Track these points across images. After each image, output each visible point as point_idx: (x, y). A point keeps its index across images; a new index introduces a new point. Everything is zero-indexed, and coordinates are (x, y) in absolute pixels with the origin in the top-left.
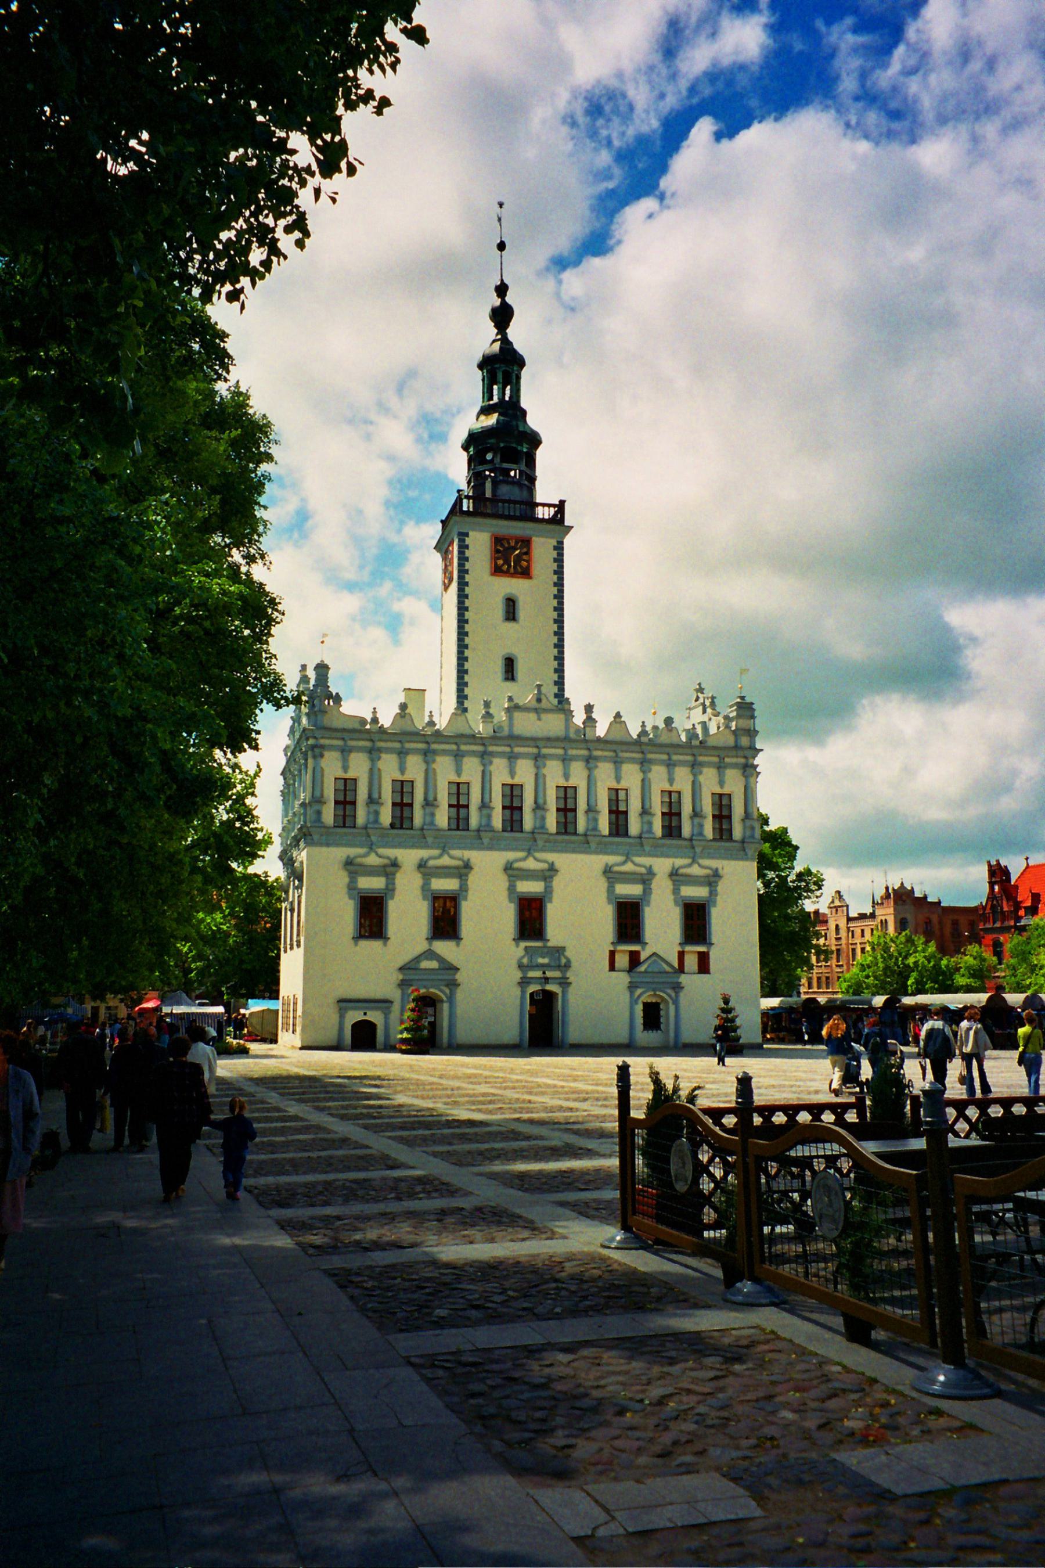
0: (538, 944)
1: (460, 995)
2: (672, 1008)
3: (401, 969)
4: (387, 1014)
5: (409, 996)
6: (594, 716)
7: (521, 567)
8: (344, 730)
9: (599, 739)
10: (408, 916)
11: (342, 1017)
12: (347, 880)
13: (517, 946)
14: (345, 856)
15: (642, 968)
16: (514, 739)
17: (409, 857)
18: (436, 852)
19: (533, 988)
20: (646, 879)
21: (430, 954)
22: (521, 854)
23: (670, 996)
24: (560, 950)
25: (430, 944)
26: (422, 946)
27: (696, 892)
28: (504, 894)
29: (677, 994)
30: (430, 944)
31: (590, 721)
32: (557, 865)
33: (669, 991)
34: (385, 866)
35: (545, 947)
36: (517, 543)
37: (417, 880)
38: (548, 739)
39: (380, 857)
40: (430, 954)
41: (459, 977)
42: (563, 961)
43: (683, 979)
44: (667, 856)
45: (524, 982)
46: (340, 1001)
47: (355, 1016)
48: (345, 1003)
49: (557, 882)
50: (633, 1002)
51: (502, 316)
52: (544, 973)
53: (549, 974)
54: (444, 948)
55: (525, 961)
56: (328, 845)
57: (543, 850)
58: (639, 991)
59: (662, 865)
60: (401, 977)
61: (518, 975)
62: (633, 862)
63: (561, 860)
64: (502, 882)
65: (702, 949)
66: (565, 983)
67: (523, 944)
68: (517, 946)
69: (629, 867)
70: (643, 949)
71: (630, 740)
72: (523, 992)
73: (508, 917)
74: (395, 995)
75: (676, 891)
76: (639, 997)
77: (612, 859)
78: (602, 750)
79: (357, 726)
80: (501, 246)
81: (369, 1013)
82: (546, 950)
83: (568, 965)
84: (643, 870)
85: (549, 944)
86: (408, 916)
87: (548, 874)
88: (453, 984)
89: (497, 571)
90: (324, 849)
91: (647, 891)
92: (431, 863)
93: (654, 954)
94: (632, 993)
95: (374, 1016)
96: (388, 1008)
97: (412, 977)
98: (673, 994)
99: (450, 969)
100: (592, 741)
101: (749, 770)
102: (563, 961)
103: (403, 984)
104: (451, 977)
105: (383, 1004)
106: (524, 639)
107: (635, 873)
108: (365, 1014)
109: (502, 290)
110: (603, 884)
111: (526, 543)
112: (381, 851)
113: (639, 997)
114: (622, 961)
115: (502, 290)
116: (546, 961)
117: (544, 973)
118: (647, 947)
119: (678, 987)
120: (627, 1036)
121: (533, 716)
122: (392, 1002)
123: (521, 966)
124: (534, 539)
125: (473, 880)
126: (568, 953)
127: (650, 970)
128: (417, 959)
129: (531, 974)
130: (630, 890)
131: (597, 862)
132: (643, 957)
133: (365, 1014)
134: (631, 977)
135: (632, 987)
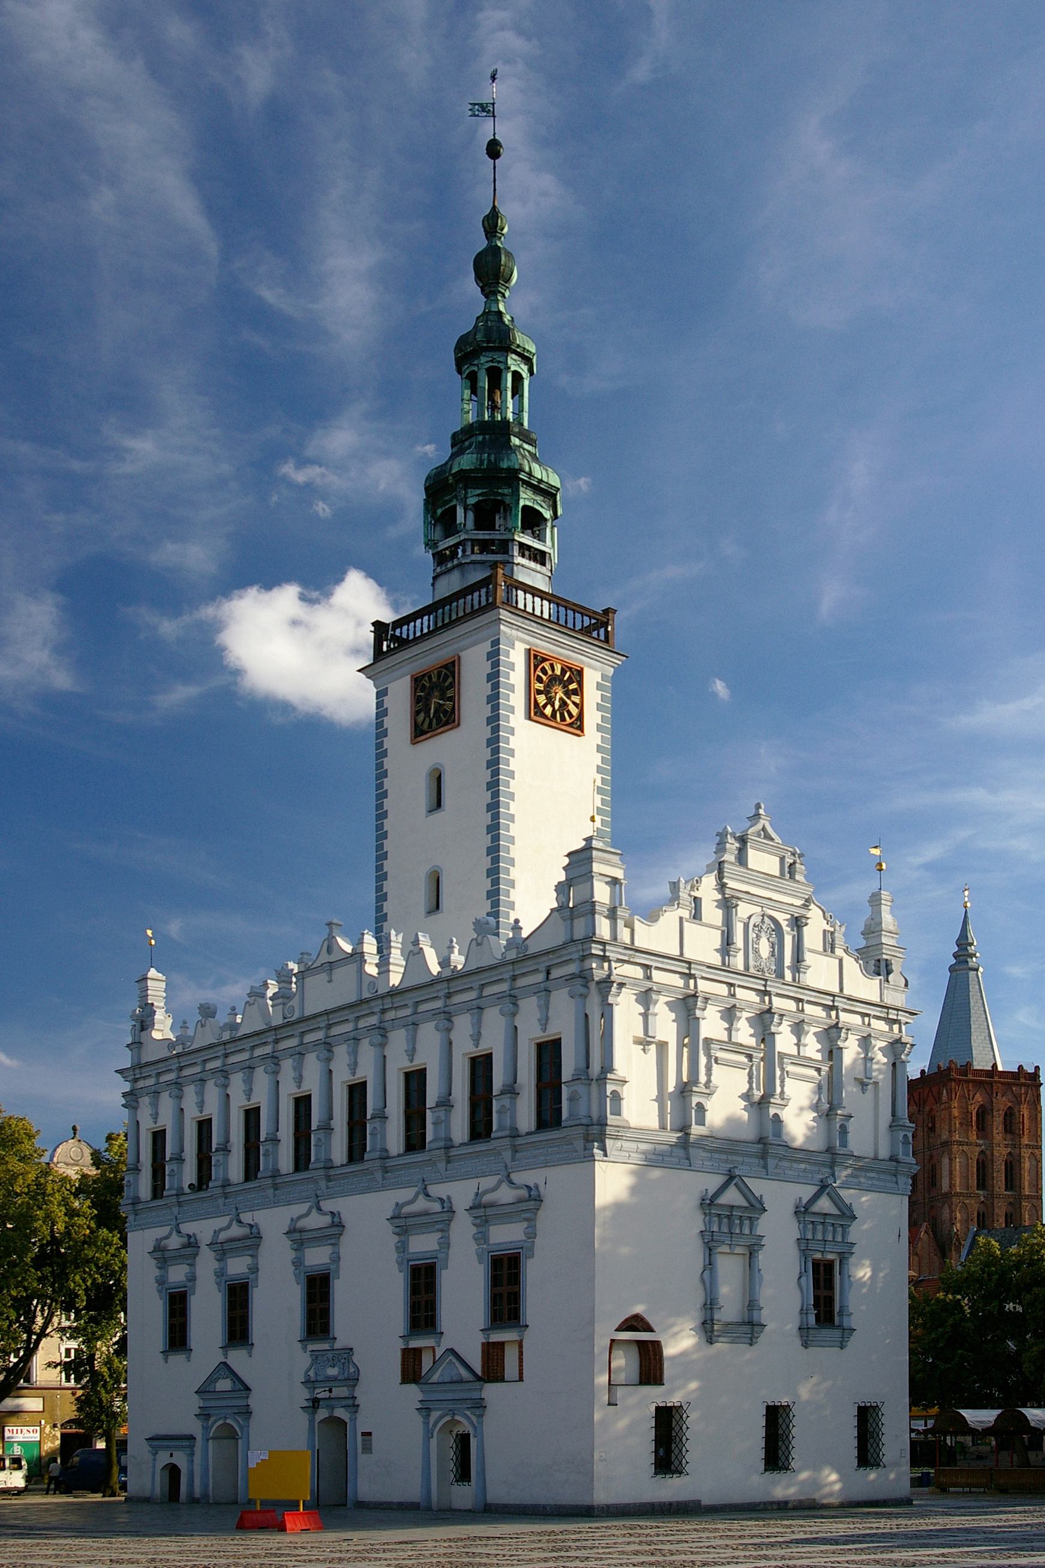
0: (326, 1346)
15: (435, 1378)
19: (322, 1414)
21: (225, 1368)
22: (303, 1208)
32: (346, 1218)
34: (184, 1247)
36: (440, 673)
42: (352, 1370)
43: (491, 1392)
47: (164, 1458)
48: (158, 1441)
50: (428, 1434)
54: (237, 1358)
57: (330, 1197)
58: (435, 1415)
59: (461, 1193)
61: (303, 1395)
66: (354, 1407)
68: (305, 1349)
69: (421, 1204)
72: (312, 1421)
74: (194, 1427)
75: (481, 1237)
77: (404, 1194)
81: (174, 1453)
82: (330, 1355)
84: (437, 1207)
85: (338, 1345)
89: (420, 732)
92: (223, 1236)
93: (452, 1351)
95: (180, 1459)
96: (192, 1447)
97: (213, 1403)
98: (474, 1419)
102: (352, 1370)
103: (204, 1415)
104: (243, 1403)
107: (426, 1213)
108: (171, 1455)
117: (330, 1391)
119: (479, 1406)
122: (192, 1438)
123: (308, 1382)
128: (212, 1379)
130: (423, 1244)
133: (171, 1455)
135: (425, 1410)
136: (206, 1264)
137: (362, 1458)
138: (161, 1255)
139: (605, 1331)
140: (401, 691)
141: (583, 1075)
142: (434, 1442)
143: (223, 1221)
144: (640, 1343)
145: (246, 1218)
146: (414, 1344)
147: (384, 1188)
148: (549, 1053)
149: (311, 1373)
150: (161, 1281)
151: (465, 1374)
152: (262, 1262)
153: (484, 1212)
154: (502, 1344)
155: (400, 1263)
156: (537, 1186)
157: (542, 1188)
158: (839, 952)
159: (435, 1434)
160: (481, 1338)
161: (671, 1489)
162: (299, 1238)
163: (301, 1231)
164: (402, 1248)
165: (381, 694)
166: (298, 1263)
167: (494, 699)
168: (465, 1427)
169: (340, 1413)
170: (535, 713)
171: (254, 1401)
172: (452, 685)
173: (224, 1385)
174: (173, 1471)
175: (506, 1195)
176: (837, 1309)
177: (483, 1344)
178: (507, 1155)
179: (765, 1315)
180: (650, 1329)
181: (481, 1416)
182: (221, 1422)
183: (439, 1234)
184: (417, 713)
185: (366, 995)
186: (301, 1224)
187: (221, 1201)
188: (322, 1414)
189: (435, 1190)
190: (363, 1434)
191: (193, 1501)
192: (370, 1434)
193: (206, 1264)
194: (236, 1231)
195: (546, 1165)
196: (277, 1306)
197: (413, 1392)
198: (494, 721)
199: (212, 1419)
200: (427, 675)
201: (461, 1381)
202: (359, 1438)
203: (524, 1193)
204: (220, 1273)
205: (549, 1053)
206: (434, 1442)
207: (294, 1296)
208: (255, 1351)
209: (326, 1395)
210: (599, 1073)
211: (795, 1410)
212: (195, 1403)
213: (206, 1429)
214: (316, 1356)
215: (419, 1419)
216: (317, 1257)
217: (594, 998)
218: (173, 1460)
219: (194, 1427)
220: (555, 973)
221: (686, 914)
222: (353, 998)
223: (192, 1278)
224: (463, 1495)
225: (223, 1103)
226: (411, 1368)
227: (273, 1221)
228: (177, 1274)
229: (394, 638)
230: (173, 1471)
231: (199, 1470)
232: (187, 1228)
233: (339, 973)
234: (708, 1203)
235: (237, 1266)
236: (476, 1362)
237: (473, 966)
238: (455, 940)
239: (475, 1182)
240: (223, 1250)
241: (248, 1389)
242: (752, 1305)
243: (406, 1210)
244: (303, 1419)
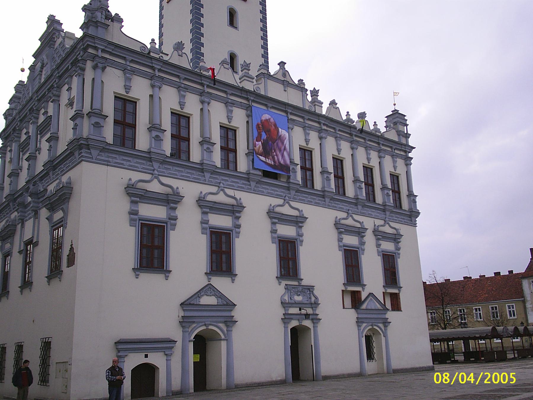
1: (237, 333)
2: (383, 339)
3: (182, 304)
5: (190, 333)
6: (319, 98)
13: (280, 283)
14: (126, 182)
15: (364, 306)
17: (190, 190)
18: (214, 189)
19: (294, 323)
20: (360, 232)
21: (209, 289)
22: (281, 202)
23: (381, 329)
24: (310, 289)
25: (209, 280)
26: (203, 281)
29: (386, 326)
30: (209, 280)
31: (316, 102)
33: (381, 325)
35: (300, 285)
37: (196, 215)
39: (162, 184)
40: (209, 289)
41: (236, 314)
46: (115, 343)
48: (124, 346)
49: (306, 230)
52: (300, 310)
54: (221, 283)
55: (286, 298)
56: (107, 164)
57: (294, 200)
58: (364, 325)
60: (182, 314)
61: (280, 312)
64: (266, 224)
65: (395, 291)
66: (315, 320)
67: (284, 283)
68: (280, 283)
70: (363, 289)
72: (286, 328)
73: (270, 254)
76: (364, 330)
78: (327, 126)
81: (149, 355)
83: (315, 305)
84: (358, 225)
85: (304, 283)
87: (299, 219)
88: (230, 322)
90: (103, 168)
91: (363, 243)
92: (210, 198)
93: (371, 294)
94: (359, 326)
95: (156, 359)
99: (227, 305)
101: (408, 161)
102: (313, 299)
105: (165, 345)
108: (146, 356)
110: (333, 234)
112: (164, 180)
113: (364, 330)
114: (348, 301)
119: (386, 323)
120: (359, 367)
121: (281, 87)
123: (284, 304)
125: (245, 220)
127: (370, 308)
128: (198, 294)
132: (364, 296)
133: (146, 356)
134: (358, 313)
135: (359, 322)
147: (329, 207)
149: (286, 298)
164: (340, 240)
169: (307, 323)
173: (208, 300)
186: (278, 209)
208: (237, 279)
212: (177, 313)
214: (287, 287)
215: (356, 328)
219: (175, 332)
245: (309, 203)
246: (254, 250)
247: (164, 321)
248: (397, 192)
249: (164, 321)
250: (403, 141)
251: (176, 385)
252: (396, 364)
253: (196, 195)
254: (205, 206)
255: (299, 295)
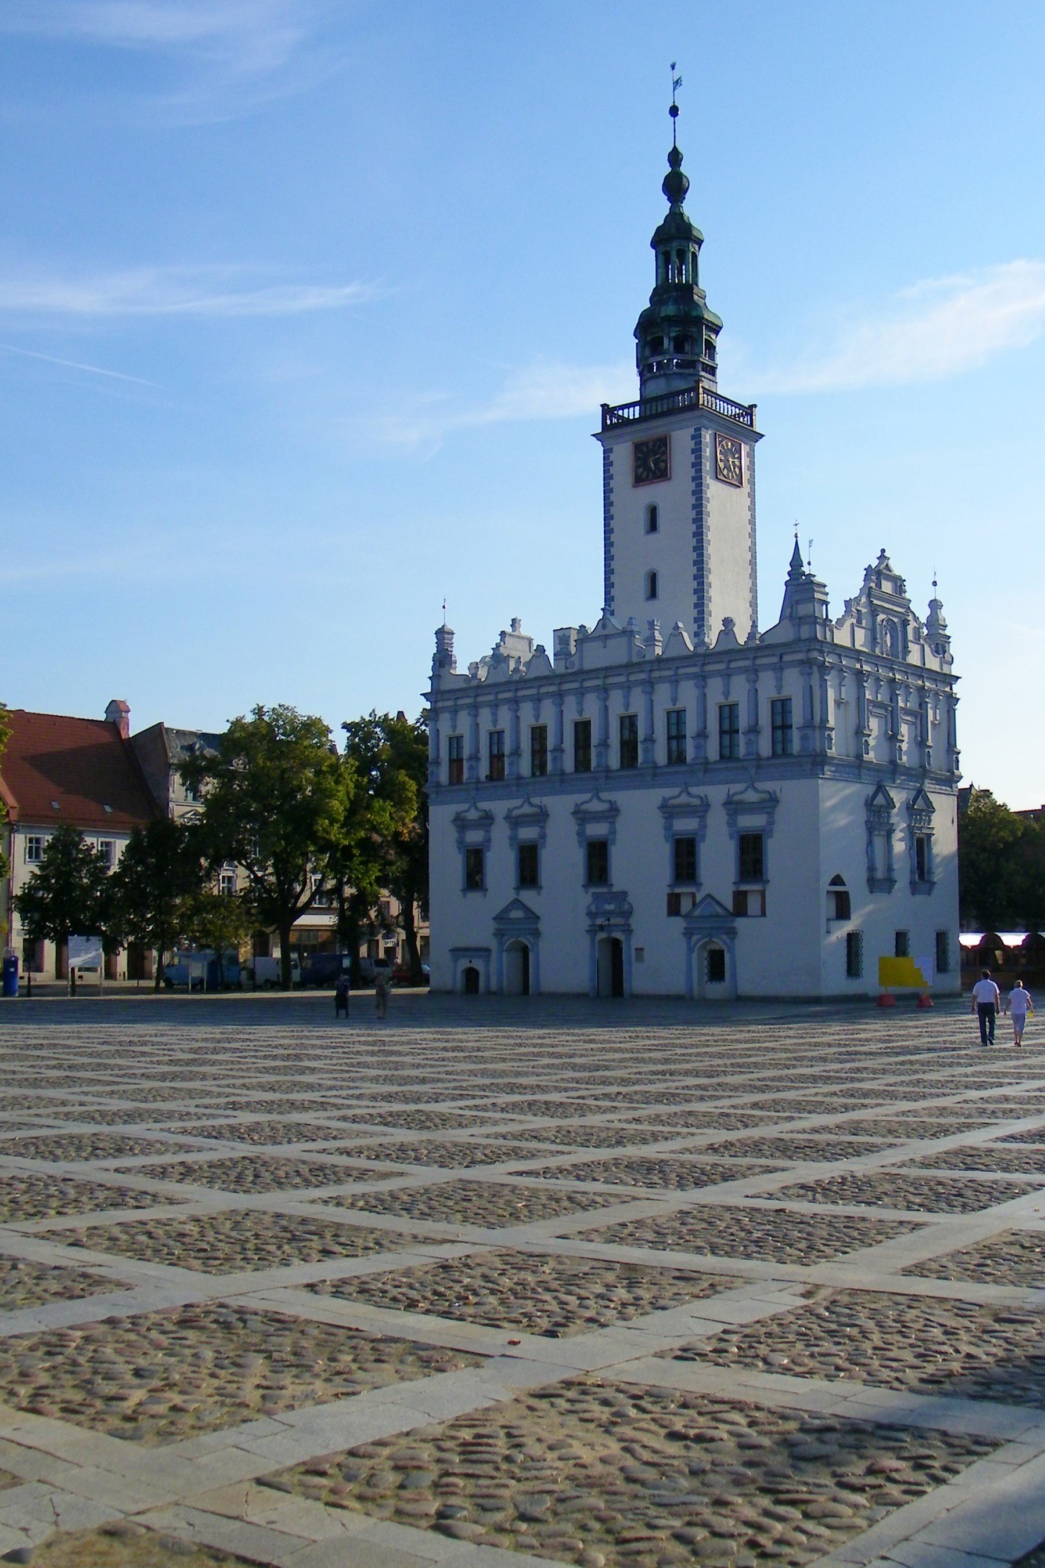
0: (605, 890)
4: (488, 962)
7: (660, 470)
8: (449, 691)
9: (659, 660)
10: (501, 865)
11: (455, 965)
12: (508, 832)
15: (697, 913)
16: (583, 674)
17: (499, 807)
19: (602, 935)
21: (517, 904)
22: (587, 796)
24: (625, 894)
25: (518, 894)
26: (512, 895)
27: (751, 822)
28: (574, 840)
29: (733, 939)
30: (518, 894)
33: (724, 937)
34: (481, 818)
36: (654, 445)
38: (606, 669)
40: (517, 904)
42: (626, 907)
43: (740, 923)
44: (719, 783)
45: (593, 930)
48: (458, 952)
50: (691, 950)
51: (675, 187)
53: (613, 921)
54: (528, 897)
55: (593, 908)
57: (607, 790)
58: (695, 938)
59: (716, 793)
60: (497, 926)
62: (689, 794)
63: (623, 798)
64: (572, 826)
66: (628, 931)
69: (684, 799)
70: (698, 891)
71: (684, 653)
72: (593, 940)
74: (492, 943)
75: (732, 823)
76: (696, 944)
79: (464, 685)
80: (674, 111)
83: (628, 914)
85: (614, 889)
86: (501, 865)
88: (536, 933)
89: (639, 480)
91: (703, 826)
92: (516, 813)
93: (709, 896)
95: (478, 964)
96: (489, 956)
98: (728, 941)
100: (651, 662)
102: (626, 907)
103: (499, 934)
104: (534, 926)
106: (667, 551)
107: (688, 805)
109: (675, 158)
110: (659, 821)
111: (662, 444)
113: (696, 944)
115: (675, 158)
116: (612, 907)
117: (609, 920)
118: (702, 888)
119: (732, 932)
122: (488, 950)
123: (590, 914)
124: (673, 434)
126: (630, 899)
129: (599, 921)
130: (685, 825)
131: (655, 796)
132: (698, 898)
135: (688, 933)
136: (500, 832)
137: (636, 966)
138: (461, 823)
139: (825, 885)
140: (624, 452)
141: (809, 725)
142: (695, 955)
143: (518, 802)
144: (836, 892)
145: (535, 800)
146: (677, 890)
147: (653, 787)
148: (781, 707)
150: (461, 842)
151: (719, 910)
152: (548, 831)
153: (734, 807)
154: (745, 892)
155: (666, 838)
156: (774, 791)
157: (778, 794)
158: (922, 641)
159: (696, 949)
160: (733, 888)
161: (854, 987)
162: (582, 816)
163: (585, 812)
164: (668, 827)
165: (607, 453)
166: (580, 834)
167: (697, 465)
168: (718, 943)
170: (717, 475)
171: (542, 926)
172: (664, 453)
174: (471, 975)
175: (751, 796)
176: (926, 869)
177: (734, 892)
178: (753, 771)
179: (896, 875)
180: (843, 884)
181: (734, 938)
182: (512, 940)
183: (698, 820)
184: (637, 468)
185: (635, 660)
186: (584, 807)
187: (514, 789)
188: (602, 935)
189: (693, 790)
190: (636, 949)
191: (489, 993)
192: (642, 949)
193: (500, 832)
194: (527, 809)
195: (782, 778)
196: (563, 859)
197: (678, 924)
198: (698, 479)
199: (505, 938)
200: (646, 444)
201: (717, 916)
202: (633, 952)
203: (766, 796)
204: (513, 838)
205: (781, 707)
206: (695, 955)
207: (578, 857)
209: (607, 923)
210: (816, 725)
211: (910, 935)
212: (492, 926)
213: (501, 944)
214: (596, 896)
216: (597, 830)
217: (816, 675)
218: (472, 965)
220: (786, 658)
221: (854, 621)
222: (624, 660)
223: (488, 840)
224: (716, 990)
225: (516, 724)
226: (674, 907)
227: (561, 806)
228: (474, 837)
229: (619, 417)
230: (471, 975)
231: (496, 972)
232: (484, 805)
233: (611, 642)
234: (869, 803)
235: (528, 833)
236: (730, 905)
237: (723, 648)
238: (680, 625)
239: (728, 786)
240: (515, 822)
241: (538, 917)
242: (890, 869)
243: (671, 802)
244: (585, 941)
245: (626, 788)
246: (563, 859)
247: (483, 935)
248: (782, 727)
249: (483, 935)
250: (805, 632)
251: (494, 985)
252: (746, 988)
253: (504, 812)
254: (515, 822)
255: (610, 904)
